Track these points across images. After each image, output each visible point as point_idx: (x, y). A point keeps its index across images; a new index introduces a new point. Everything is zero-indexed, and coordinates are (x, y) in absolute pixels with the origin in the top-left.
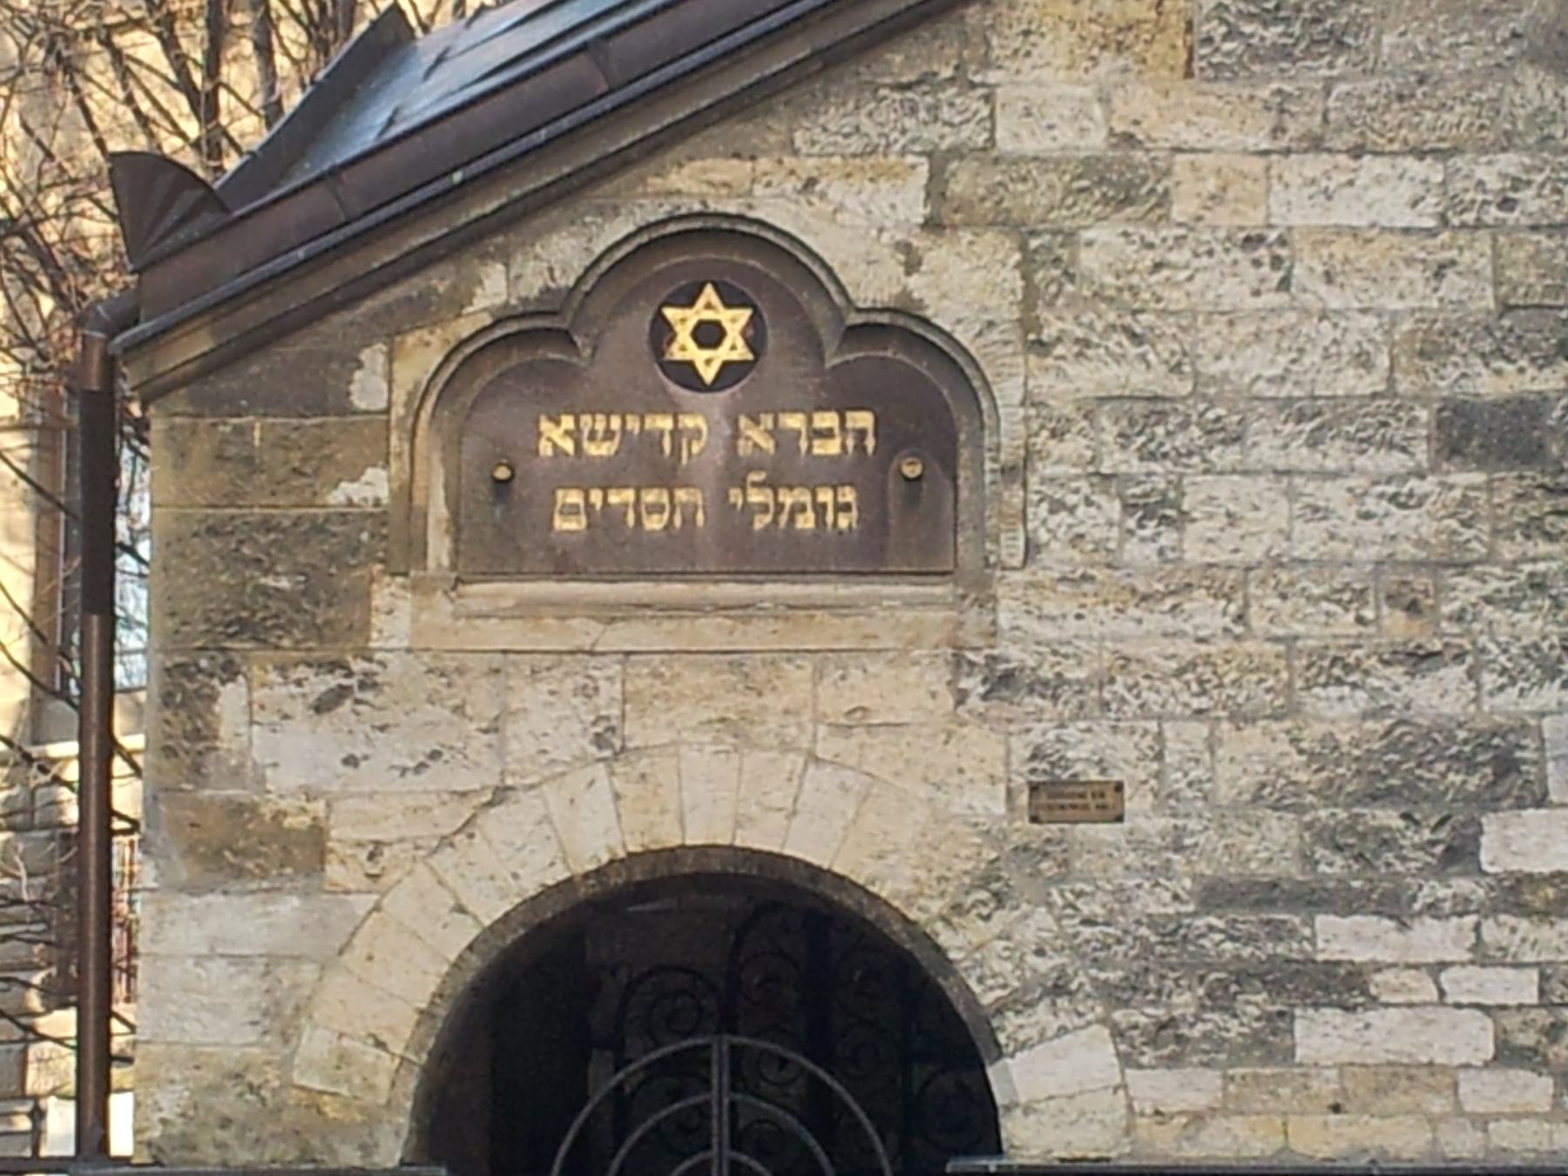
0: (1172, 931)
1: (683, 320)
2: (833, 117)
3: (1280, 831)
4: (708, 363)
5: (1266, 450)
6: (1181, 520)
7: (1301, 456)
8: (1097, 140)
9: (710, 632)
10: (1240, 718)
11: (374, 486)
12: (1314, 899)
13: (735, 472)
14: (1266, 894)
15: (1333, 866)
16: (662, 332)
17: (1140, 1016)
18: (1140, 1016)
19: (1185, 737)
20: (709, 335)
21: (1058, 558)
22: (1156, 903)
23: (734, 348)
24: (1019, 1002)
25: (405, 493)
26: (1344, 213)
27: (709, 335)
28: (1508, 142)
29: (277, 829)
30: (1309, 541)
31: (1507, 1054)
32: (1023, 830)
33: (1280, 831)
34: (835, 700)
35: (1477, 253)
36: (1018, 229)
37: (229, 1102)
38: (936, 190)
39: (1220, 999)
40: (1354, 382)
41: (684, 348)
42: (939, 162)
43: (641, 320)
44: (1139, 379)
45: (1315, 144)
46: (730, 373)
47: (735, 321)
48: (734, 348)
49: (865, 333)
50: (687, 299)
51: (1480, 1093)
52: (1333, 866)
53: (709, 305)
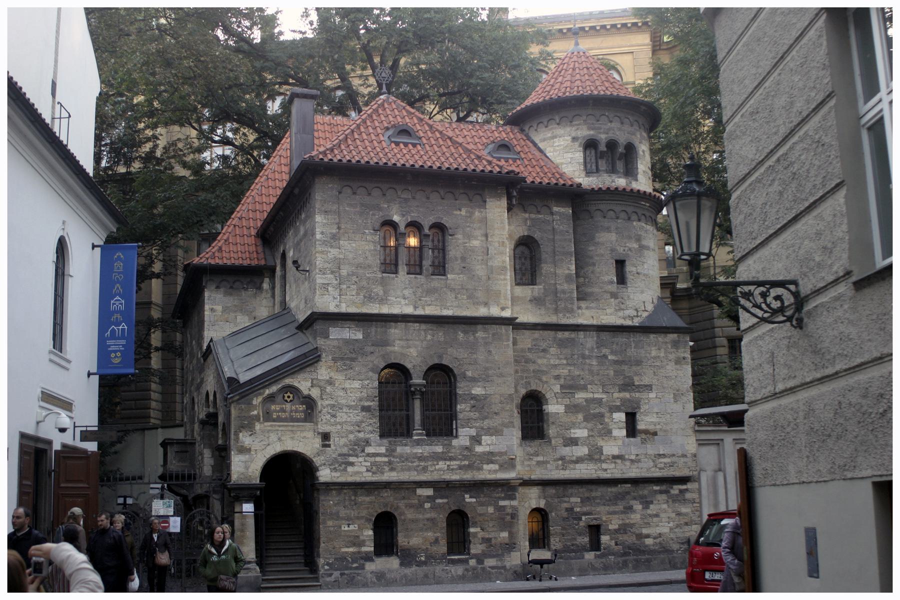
0: (335, 458)
1: (286, 395)
2: (302, 375)
3: (346, 448)
4: (289, 400)
5: (344, 410)
6: (336, 417)
7: (348, 411)
8: (328, 378)
9: (290, 428)
10: (342, 437)
11: (255, 413)
12: (349, 455)
13: (291, 411)
14: (344, 455)
15: (351, 452)
16: (284, 397)
17: (333, 467)
18: (333, 467)
19: (337, 439)
20: (289, 397)
21: (324, 421)
22: (334, 456)
23: (291, 398)
24: (321, 466)
25: (258, 413)
26: (352, 386)
27: (289, 397)
28: (368, 379)
29: (246, 448)
30: (349, 419)
31: (368, 471)
32: (321, 448)
33: (346, 448)
34: (302, 435)
35: (365, 391)
36: (320, 387)
37: (242, 476)
38: (312, 383)
39: (340, 465)
40: (353, 403)
41: (286, 398)
42: (312, 380)
43: (281, 395)
44: (332, 403)
45: (349, 379)
46: (291, 401)
47: (291, 396)
48: (291, 398)
49: (305, 397)
50: (287, 393)
51: (365, 474)
52: (351, 452)
53: (289, 394)
